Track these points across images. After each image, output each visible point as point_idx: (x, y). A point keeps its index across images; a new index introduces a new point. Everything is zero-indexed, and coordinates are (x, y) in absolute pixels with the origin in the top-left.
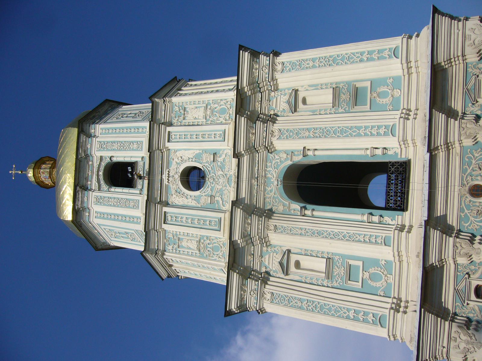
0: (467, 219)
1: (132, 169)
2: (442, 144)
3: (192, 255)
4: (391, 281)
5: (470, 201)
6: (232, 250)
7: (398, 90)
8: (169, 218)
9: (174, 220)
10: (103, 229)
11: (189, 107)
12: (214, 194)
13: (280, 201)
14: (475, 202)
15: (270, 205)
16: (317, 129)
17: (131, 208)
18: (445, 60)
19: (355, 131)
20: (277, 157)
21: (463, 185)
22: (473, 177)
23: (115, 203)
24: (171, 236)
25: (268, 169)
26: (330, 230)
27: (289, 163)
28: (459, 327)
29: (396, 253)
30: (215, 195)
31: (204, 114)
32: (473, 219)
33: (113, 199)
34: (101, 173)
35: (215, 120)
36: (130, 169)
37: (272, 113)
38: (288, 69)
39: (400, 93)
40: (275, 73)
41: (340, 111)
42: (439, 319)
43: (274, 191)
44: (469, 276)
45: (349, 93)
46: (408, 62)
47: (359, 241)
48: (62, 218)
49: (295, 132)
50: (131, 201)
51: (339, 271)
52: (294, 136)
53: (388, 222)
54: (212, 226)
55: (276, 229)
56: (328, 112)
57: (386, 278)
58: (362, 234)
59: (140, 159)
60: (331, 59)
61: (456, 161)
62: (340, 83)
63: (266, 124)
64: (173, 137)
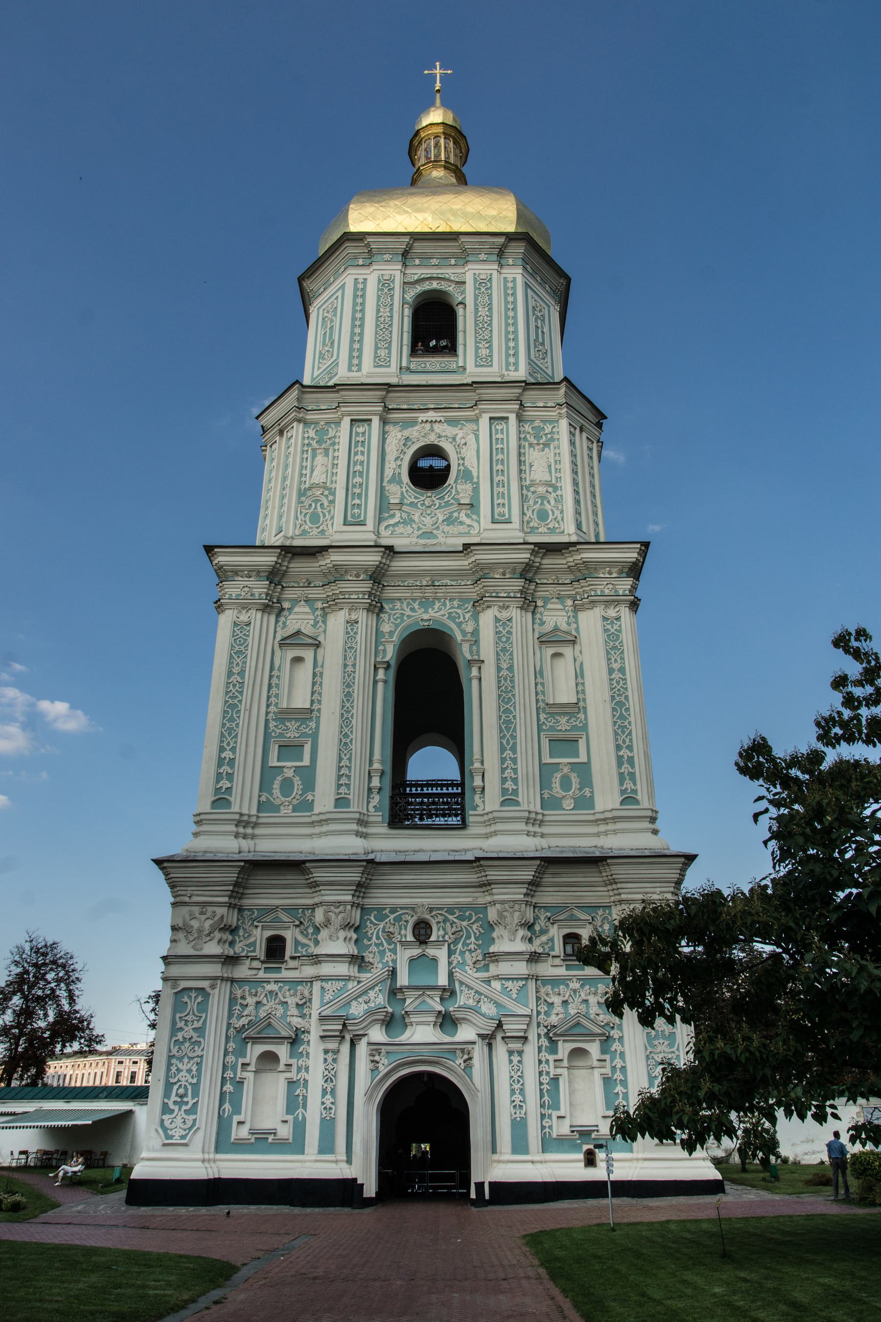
0: (381, 918)
1: (445, 347)
2: (489, 878)
3: (301, 475)
4: (284, 811)
5: (407, 921)
6: (314, 550)
7: (573, 805)
9: (358, 439)
10: (335, 297)
11: (550, 453)
12: (405, 508)
13: (397, 626)
14: (406, 929)
15: (391, 609)
16: (512, 681)
17: (376, 353)
18: (614, 876)
19: (508, 744)
20: (467, 616)
21: (431, 910)
22: (442, 924)
23: (382, 319)
24: (331, 433)
25: (447, 602)
26: (354, 711)
27: (459, 637)
28: (222, 917)
29: (322, 817)
30: (404, 511)
31: (538, 481)
32: (381, 926)
33: (388, 314)
34: (435, 285)
35: (528, 502)
36: (443, 343)
37: (540, 603)
38: (609, 627)
39: (568, 808)
40: (602, 607)
41: (541, 716)
42: (231, 888)
43: (414, 614)
44: (297, 926)
45: (568, 728)
46: (615, 819)
47: (340, 759)
48: (351, 206)
49: (506, 645)
50: (387, 351)
51: (292, 731)
52: (501, 644)
53: (371, 800)
54: (352, 509)
55: (352, 625)
56: (541, 697)
57: (287, 804)
58: (350, 763)
59: (461, 364)
60: (623, 699)
61: (464, 898)
62: (585, 713)
63: (519, 596)
64: (499, 427)
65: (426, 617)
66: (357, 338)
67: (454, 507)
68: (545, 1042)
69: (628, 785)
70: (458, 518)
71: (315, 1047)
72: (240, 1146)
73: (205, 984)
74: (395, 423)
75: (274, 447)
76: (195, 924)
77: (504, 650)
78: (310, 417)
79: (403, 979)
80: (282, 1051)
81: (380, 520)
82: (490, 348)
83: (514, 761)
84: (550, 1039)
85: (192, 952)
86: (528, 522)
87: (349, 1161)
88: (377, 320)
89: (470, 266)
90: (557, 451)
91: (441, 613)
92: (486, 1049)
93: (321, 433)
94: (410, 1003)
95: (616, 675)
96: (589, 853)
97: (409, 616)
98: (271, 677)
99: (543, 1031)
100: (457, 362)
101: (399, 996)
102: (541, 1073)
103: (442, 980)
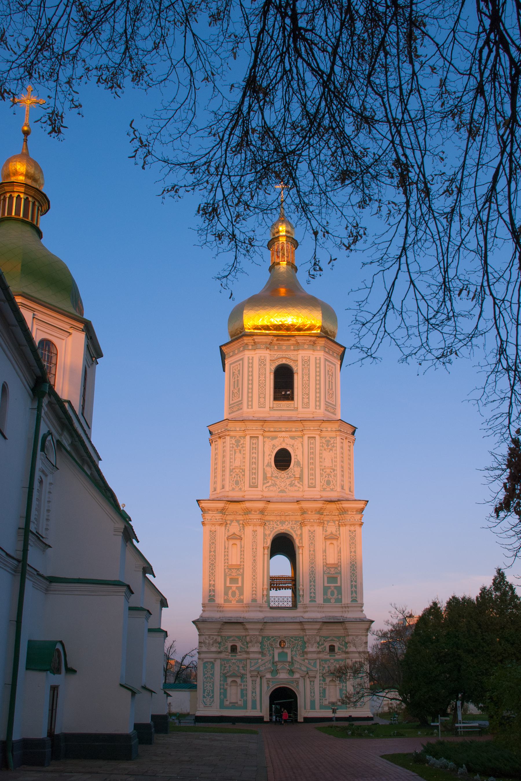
3: (230, 462)
8: (254, 442)
13: (271, 531)
16: (314, 556)
17: (259, 400)
20: (298, 527)
21: (285, 637)
24: (242, 442)
27: (295, 536)
34: (284, 361)
36: (288, 393)
37: (326, 523)
47: (253, 585)
48: (245, 311)
51: (234, 573)
59: (296, 406)
62: (341, 567)
64: (312, 442)
65: (282, 528)
66: (250, 391)
67: (293, 479)
68: (322, 678)
69: (354, 595)
70: (294, 484)
71: (249, 680)
72: (227, 707)
73: (213, 660)
74: (268, 437)
75: (216, 443)
76: (207, 641)
77: (312, 543)
78: (232, 433)
79: (276, 659)
80: (239, 680)
81: (264, 484)
82: (308, 398)
83: (314, 586)
84: (323, 677)
85: (207, 650)
86: (323, 486)
87: (261, 711)
88: (259, 382)
89: (300, 352)
90: (335, 452)
91: (288, 526)
92: (303, 680)
93: (238, 441)
94: (279, 666)
95: (353, 554)
96: (338, 619)
97: (276, 528)
98: (225, 552)
99: (321, 675)
100: (294, 404)
101: (275, 664)
102: (320, 687)
103: (289, 659)
